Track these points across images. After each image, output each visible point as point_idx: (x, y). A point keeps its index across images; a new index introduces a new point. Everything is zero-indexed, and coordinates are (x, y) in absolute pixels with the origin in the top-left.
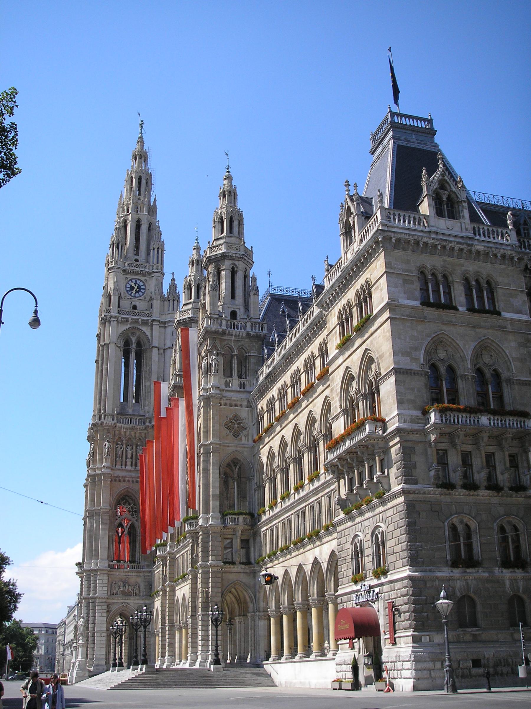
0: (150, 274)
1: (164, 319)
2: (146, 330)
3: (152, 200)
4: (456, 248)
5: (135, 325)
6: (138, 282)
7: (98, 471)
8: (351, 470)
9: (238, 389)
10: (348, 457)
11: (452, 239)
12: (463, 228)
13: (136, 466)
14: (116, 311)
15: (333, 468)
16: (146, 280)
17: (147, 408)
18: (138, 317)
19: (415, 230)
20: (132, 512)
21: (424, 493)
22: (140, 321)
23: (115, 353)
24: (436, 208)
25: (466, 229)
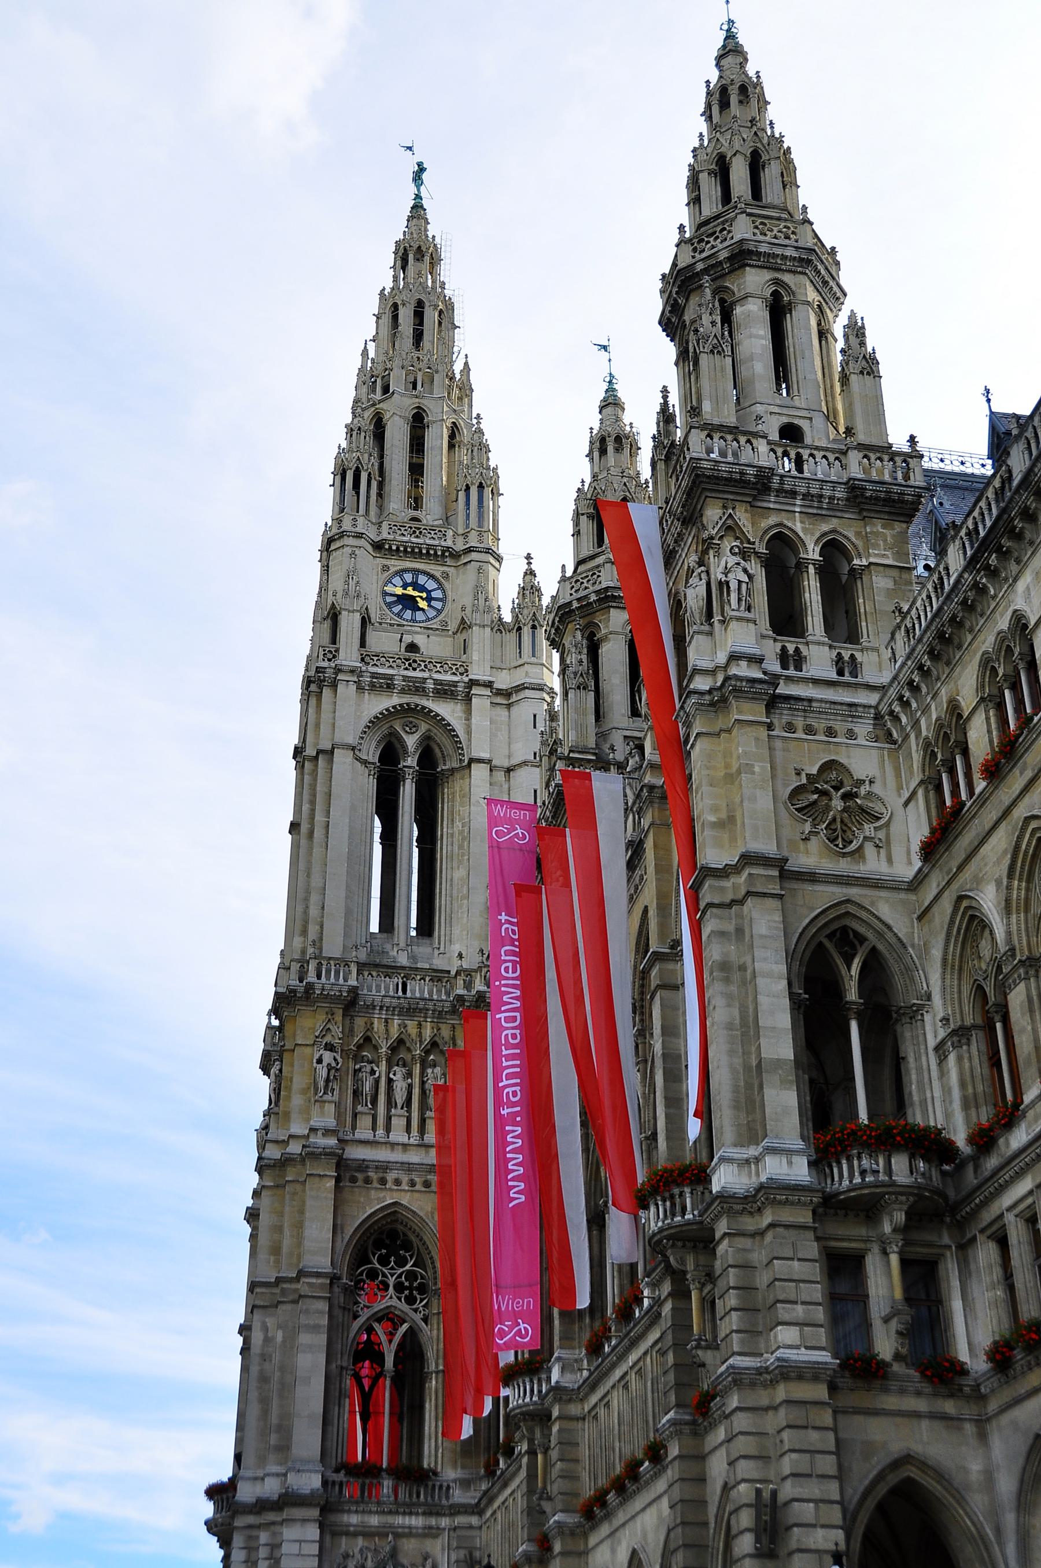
0: (456, 556)
2: (448, 711)
3: (458, 367)
5: (416, 700)
7: (295, 1148)
9: (833, 675)
13: (422, 1130)
16: (446, 576)
18: (426, 675)
20: (411, 1288)
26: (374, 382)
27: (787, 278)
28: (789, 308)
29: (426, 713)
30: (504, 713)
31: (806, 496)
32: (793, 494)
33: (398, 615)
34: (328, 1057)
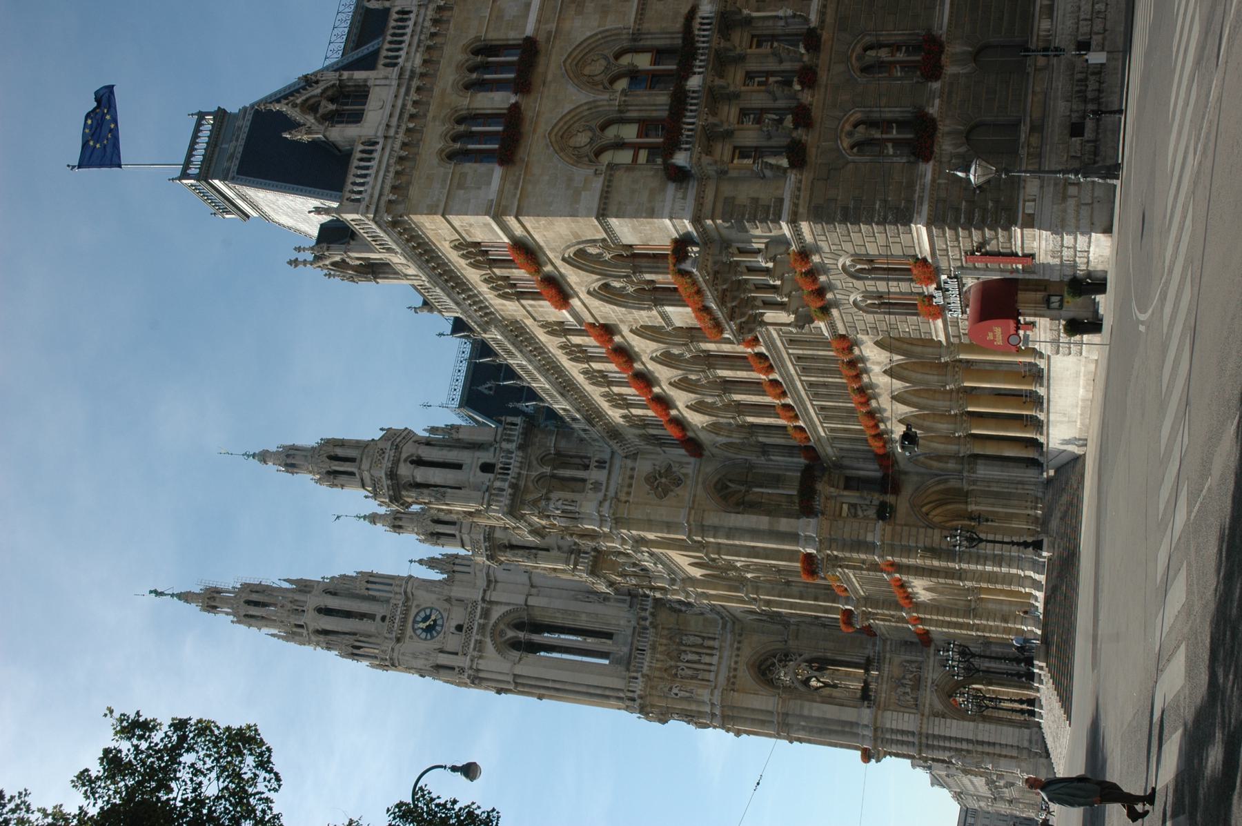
0: (407, 599)
1: (482, 583)
3: (286, 585)
4: (416, 97)
6: (419, 619)
8: (750, 302)
9: (605, 472)
10: (729, 305)
11: (400, 103)
12: (383, 82)
13: (712, 648)
14: (463, 658)
15: (745, 331)
16: (418, 606)
17: (622, 622)
19: (380, 162)
21: (799, 189)
22: (482, 621)
23: (530, 665)
24: (348, 122)
25: (386, 78)
26: (295, 633)
27: (404, 456)
28: (419, 458)
29: (496, 625)
30: (499, 585)
31: (521, 468)
32: (519, 474)
33: (438, 633)
34: (675, 690)
